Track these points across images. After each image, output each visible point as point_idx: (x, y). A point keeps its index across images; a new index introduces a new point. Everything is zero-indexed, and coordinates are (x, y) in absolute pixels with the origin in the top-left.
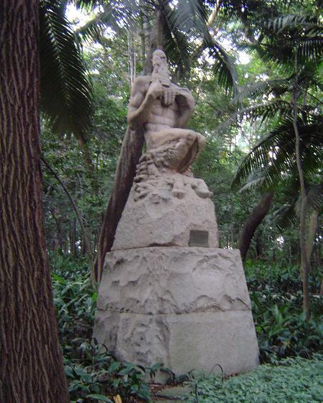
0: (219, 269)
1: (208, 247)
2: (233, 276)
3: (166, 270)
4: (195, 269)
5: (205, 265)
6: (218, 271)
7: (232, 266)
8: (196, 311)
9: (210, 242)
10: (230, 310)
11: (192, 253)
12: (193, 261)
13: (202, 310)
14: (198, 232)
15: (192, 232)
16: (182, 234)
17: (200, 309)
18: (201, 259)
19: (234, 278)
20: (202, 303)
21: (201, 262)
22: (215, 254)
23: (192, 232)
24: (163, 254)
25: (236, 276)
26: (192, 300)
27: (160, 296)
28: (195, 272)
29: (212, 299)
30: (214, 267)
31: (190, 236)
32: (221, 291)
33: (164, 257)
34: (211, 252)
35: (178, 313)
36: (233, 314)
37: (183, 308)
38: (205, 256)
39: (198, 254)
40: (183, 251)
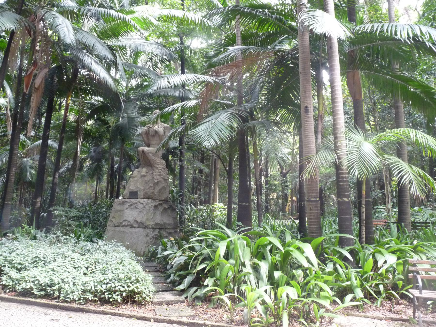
0: (138, 209)
4: (127, 209)
5: (132, 207)
8: (123, 226)
9: (138, 197)
10: (138, 227)
12: (127, 205)
13: (127, 226)
14: (132, 192)
15: (130, 192)
17: (125, 225)
20: (125, 223)
21: (131, 205)
22: (136, 202)
23: (130, 192)
26: (121, 221)
29: (129, 222)
30: (136, 208)
35: (115, 227)
36: (138, 230)
37: (117, 224)
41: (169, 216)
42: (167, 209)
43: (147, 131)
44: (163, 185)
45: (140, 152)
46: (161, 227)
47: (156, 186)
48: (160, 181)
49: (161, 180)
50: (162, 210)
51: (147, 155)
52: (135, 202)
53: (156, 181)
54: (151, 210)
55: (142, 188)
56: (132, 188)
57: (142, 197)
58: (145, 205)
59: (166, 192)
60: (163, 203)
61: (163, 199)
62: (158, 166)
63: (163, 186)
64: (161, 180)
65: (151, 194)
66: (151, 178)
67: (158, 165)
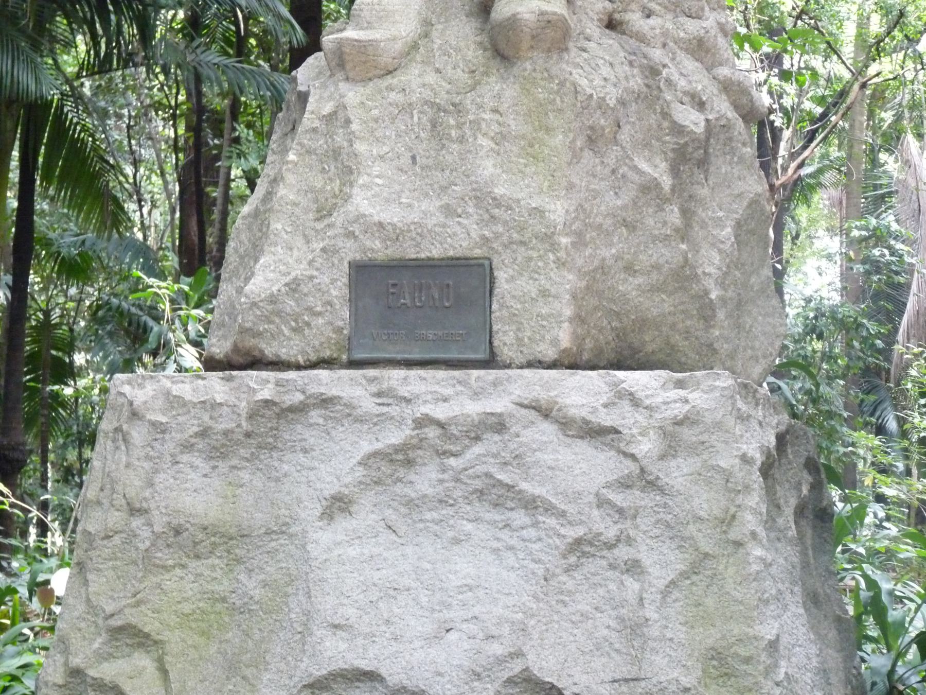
0: (531, 504)
1: (491, 362)
2: (622, 553)
3: (134, 511)
6: (520, 517)
7: (625, 484)
11: (325, 402)
16: (294, 287)
18: (394, 437)
19: (634, 568)
22: (499, 404)
24: (135, 415)
25: (647, 559)
27: (76, 661)
28: (343, 524)
31: (354, 300)
32: (497, 649)
33: (138, 434)
34: (476, 395)
38: (423, 422)
39: (369, 405)
40: (266, 393)
52: (473, 408)
56: (391, 215)
57: (564, 337)
58: (646, 447)
66: (637, 82)
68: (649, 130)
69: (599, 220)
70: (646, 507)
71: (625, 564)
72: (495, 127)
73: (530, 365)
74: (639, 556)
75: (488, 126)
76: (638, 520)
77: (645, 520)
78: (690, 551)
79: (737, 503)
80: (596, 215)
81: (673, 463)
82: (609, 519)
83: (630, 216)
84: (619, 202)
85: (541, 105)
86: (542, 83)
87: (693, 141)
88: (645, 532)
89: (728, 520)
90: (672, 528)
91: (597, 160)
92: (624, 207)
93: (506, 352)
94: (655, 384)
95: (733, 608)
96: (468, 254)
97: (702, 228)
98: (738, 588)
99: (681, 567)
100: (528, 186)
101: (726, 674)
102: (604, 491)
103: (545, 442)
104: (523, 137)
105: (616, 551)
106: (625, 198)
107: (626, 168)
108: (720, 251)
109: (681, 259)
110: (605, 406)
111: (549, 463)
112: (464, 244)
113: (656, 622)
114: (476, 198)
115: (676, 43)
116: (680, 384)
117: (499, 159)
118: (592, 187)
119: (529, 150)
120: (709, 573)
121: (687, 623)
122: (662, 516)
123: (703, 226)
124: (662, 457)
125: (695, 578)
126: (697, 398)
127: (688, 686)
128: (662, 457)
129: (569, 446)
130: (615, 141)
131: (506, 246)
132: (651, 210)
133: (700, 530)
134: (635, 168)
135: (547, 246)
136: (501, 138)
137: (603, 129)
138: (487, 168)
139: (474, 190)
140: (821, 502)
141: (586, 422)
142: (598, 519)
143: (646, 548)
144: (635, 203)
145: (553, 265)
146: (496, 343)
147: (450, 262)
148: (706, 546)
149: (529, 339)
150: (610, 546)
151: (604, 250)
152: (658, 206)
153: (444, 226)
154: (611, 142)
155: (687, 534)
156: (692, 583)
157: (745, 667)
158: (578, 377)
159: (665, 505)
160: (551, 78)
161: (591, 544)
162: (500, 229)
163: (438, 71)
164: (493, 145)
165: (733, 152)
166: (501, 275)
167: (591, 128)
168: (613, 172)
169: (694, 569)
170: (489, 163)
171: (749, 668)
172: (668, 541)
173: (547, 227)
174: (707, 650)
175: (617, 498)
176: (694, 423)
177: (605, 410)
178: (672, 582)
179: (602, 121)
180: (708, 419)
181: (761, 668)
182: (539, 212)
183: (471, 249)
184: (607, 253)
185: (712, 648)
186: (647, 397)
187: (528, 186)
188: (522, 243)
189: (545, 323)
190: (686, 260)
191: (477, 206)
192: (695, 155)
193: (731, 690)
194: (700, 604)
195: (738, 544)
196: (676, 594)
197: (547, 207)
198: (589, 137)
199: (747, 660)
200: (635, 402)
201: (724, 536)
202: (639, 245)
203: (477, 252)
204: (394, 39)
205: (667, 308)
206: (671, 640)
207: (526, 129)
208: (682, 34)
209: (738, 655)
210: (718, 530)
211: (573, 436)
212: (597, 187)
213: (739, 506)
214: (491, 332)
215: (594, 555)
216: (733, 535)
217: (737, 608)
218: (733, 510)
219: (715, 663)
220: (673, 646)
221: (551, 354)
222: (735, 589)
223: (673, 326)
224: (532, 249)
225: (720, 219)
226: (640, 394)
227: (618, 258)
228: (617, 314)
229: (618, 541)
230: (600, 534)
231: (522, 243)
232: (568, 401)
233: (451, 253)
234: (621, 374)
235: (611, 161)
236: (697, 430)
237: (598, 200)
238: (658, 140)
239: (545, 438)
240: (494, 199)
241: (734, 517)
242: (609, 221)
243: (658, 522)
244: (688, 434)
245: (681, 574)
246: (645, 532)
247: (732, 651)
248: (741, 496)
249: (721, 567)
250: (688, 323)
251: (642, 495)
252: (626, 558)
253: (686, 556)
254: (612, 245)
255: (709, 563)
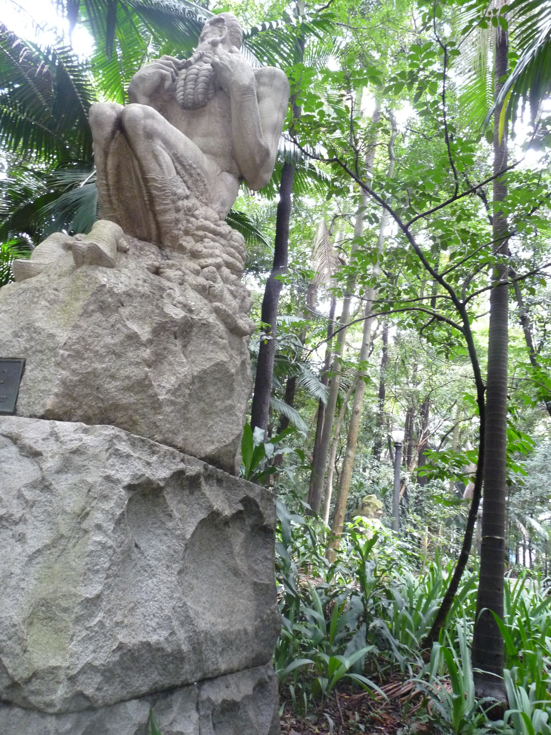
2: (20, 528)
7: (33, 486)
9: (23, 399)
19: (21, 538)
41: (236, 573)
42: (227, 522)
43: (163, 78)
44: (222, 357)
45: (100, 124)
46: (167, 682)
47: (176, 346)
48: (206, 326)
49: (212, 319)
50: (190, 529)
51: (141, 147)
53: (178, 314)
54: (98, 517)
55: (63, 336)
57: (50, 402)
59: (229, 410)
60: (209, 477)
61: (209, 449)
62: (199, 247)
63: (220, 366)
64: (212, 319)
65: (129, 399)
67: (201, 239)
68: (145, 312)
69: (98, 348)
70: (40, 501)
71: (19, 535)
72: (52, 297)
73: (31, 416)
74: (26, 531)
75: (49, 296)
76: (34, 509)
77: (38, 510)
78: (55, 532)
79: (92, 505)
80: (96, 346)
81: (64, 477)
82: (21, 506)
83: (118, 349)
84: (112, 342)
85: (78, 288)
86: (82, 278)
87: (172, 322)
88: (35, 517)
89: (84, 515)
90: (51, 516)
91: (104, 319)
92: (114, 345)
93: (21, 409)
94: (72, 429)
95: (68, 573)
96: (17, 356)
97: (169, 365)
98: (77, 560)
99: (47, 542)
100: (54, 324)
101: (49, 618)
102: (23, 489)
103: (9, 458)
104: (64, 302)
105: (17, 527)
106: (117, 340)
107: (120, 325)
108: (177, 378)
109: (144, 375)
110: (44, 439)
111: (7, 470)
112: (16, 351)
113: (17, 576)
114: (28, 328)
115: (190, 286)
116: (86, 431)
117: (48, 311)
118: (97, 331)
119: (65, 308)
120: (61, 547)
121: (39, 579)
122: (47, 508)
123: (171, 364)
124: (58, 472)
125: (53, 550)
126: (88, 439)
127: (16, 623)
128: (58, 472)
129: (20, 461)
130: (117, 311)
131: (34, 353)
132: (132, 349)
133: (64, 520)
134: (125, 326)
135: (52, 354)
136: (52, 302)
137: (109, 304)
138: (39, 314)
139: (28, 324)
140: (263, 522)
141: (31, 448)
142: (14, 506)
143: (33, 527)
144: (122, 343)
145: (53, 364)
146: (18, 404)
147: (8, 360)
148: (64, 529)
149: (33, 403)
150: (16, 523)
151: (97, 363)
152: (137, 347)
153: (11, 341)
154: (114, 311)
155: (56, 521)
156: (51, 553)
157: (63, 614)
158: (39, 423)
159: (51, 502)
160: (87, 276)
161: (7, 520)
162: (33, 343)
163: (49, 276)
164: (47, 304)
165: (210, 338)
166: (28, 368)
167: (102, 302)
168: (113, 326)
169: (53, 544)
170: (41, 312)
171: (65, 616)
172: (47, 524)
173: (55, 344)
174: (41, 599)
175: (29, 495)
176: (82, 453)
177: (42, 442)
178: (39, 551)
179: (110, 300)
180: (91, 451)
181: (73, 616)
182: (52, 336)
183: (19, 354)
184: (99, 366)
185: (44, 599)
186: (64, 436)
187: (54, 324)
188: (41, 351)
189: (41, 394)
190: (147, 376)
191: (28, 332)
192: (172, 329)
193: (50, 629)
194: (50, 568)
195: (86, 532)
196: (40, 559)
197: (58, 334)
198: (101, 307)
199: (66, 610)
200: (57, 439)
201: (78, 525)
202: (121, 365)
203: (22, 356)
204: (40, 264)
205: (132, 400)
206: (23, 589)
207: (67, 298)
208: (194, 282)
209: (59, 605)
210: (75, 521)
211: (24, 456)
212: (100, 332)
213: (93, 507)
214: (17, 397)
215: (7, 528)
216: (84, 526)
217: (70, 573)
218: (88, 509)
219: (43, 608)
220: (23, 593)
221: (41, 412)
222: (74, 560)
223: (136, 411)
224: (45, 355)
225: (183, 363)
226: (60, 435)
227: (106, 370)
228: (102, 400)
229: (20, 520)
230: (12, 515)
231: (41, 351)
232: (26, 435)
233: (10, 356)
234: (58, 423)
235: (112, 320)
236: (84, 457)
237: (100, 338)
238: (150, 317)
239: (9, 455)
240: (34, 328)
241: (87, 514)
242: (103, 350)
243: (45, 511)
244: (77, 460)
245: (45, 546)
246: (35, 517)
247: (57, 602)
248: (96, 501)
249: (70, 545)
250: (145, 410)
251: (41, 494)
252: (20, 532)
253: (52, 535)
254: (104, 363)
255: (63, 542)
